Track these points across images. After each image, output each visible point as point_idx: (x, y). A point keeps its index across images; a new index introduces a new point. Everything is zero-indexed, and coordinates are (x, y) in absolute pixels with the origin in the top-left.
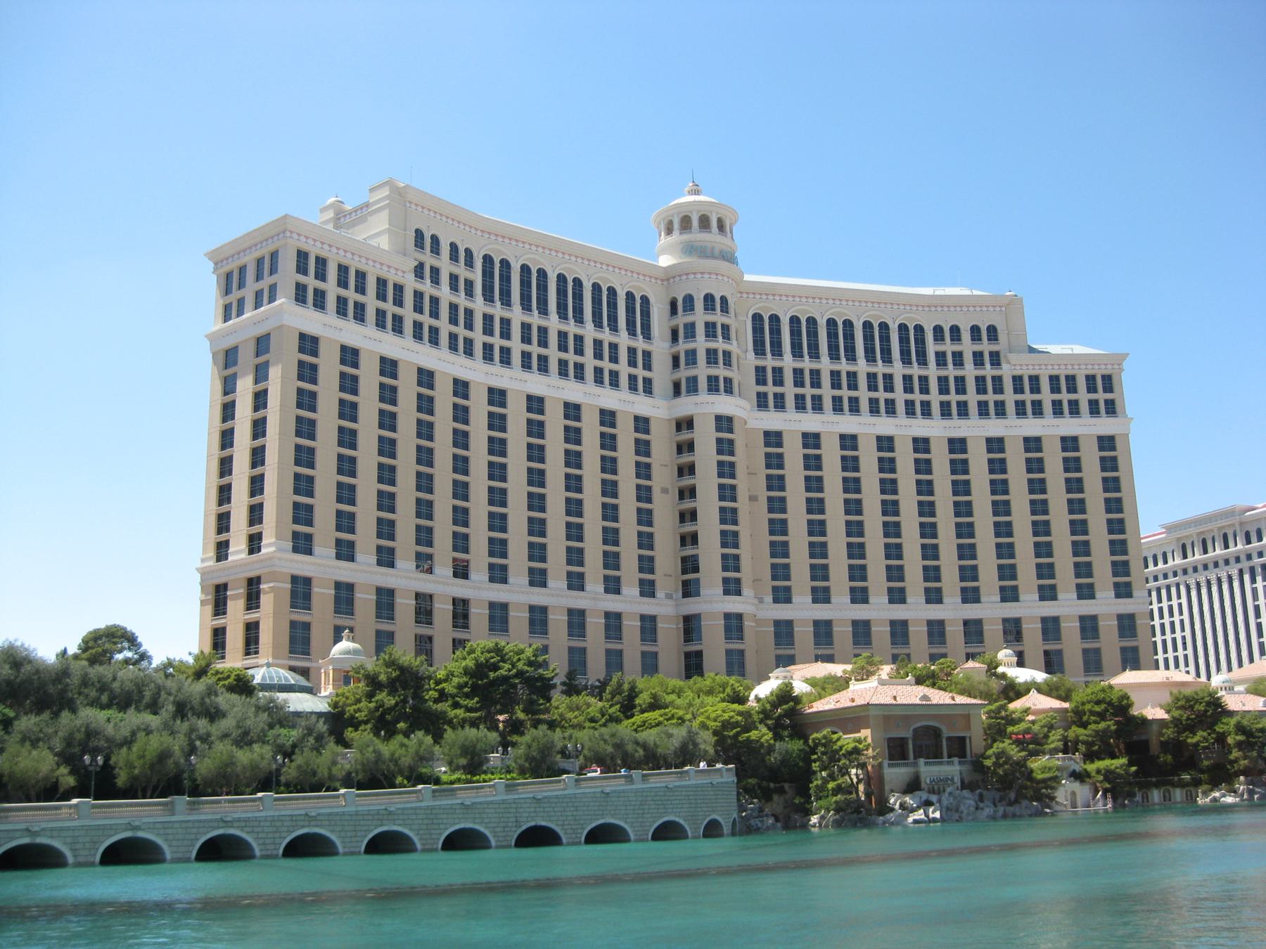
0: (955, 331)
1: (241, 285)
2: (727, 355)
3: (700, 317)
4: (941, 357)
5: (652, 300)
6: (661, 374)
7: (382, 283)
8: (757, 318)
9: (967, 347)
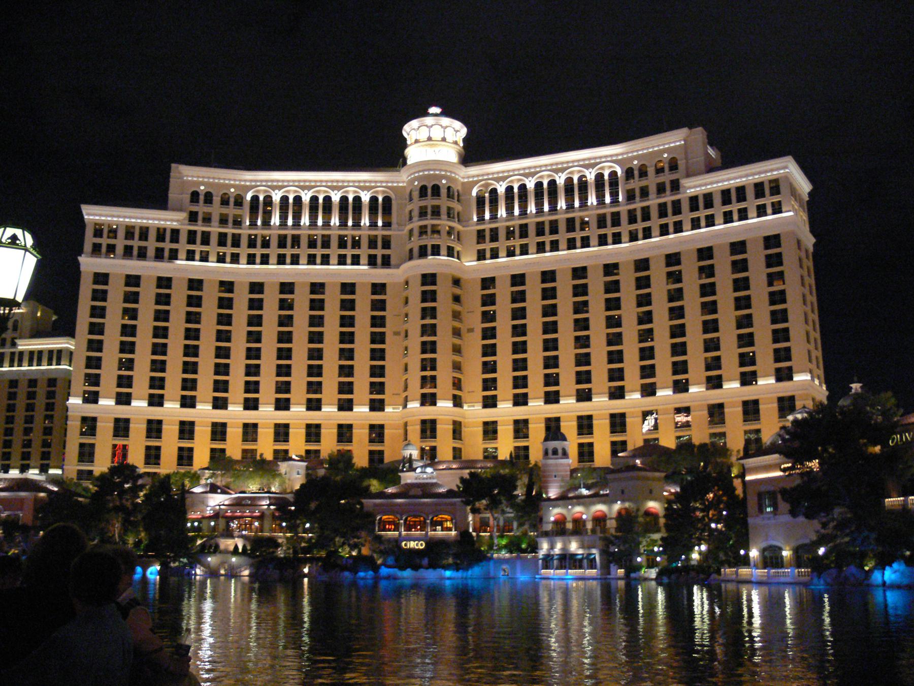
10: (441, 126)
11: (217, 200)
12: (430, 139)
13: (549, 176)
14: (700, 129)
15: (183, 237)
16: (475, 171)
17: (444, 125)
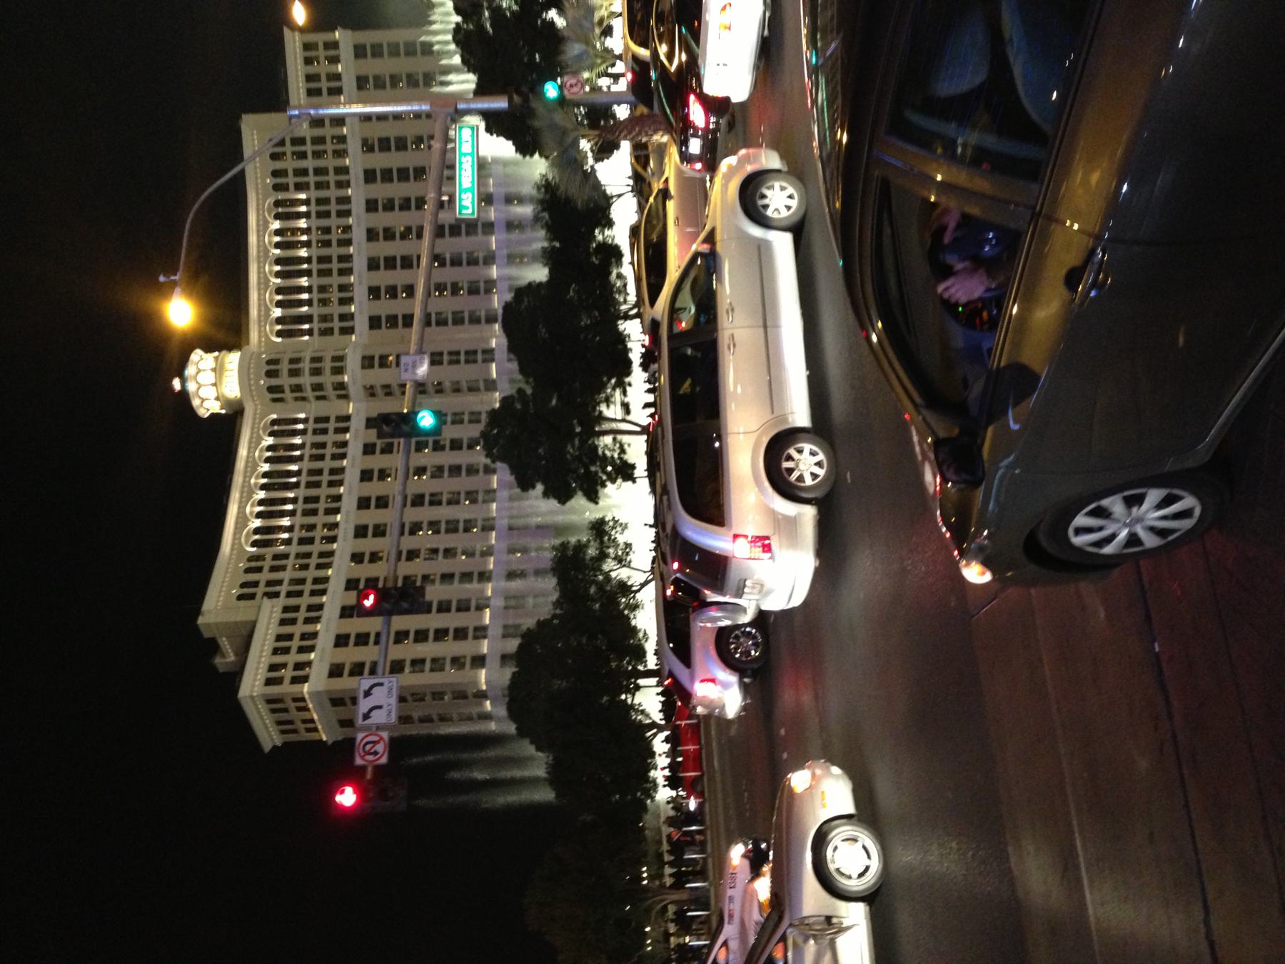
0: (275, 174)
1: (291, 722)
2: (314, 360)
3: (285, 380)
4: (299, 187)
5: (274, 416)
6: (332, 408)
7: (283, 622)
8: (279, 334)
9: (290, 164)
10: (197, 373)
11: (252, 577)
12: (214, 370)
13: (270, 265)
14: (243, 116)
15: (293, 601)
16: (254, 335)
17: (199, 358)
